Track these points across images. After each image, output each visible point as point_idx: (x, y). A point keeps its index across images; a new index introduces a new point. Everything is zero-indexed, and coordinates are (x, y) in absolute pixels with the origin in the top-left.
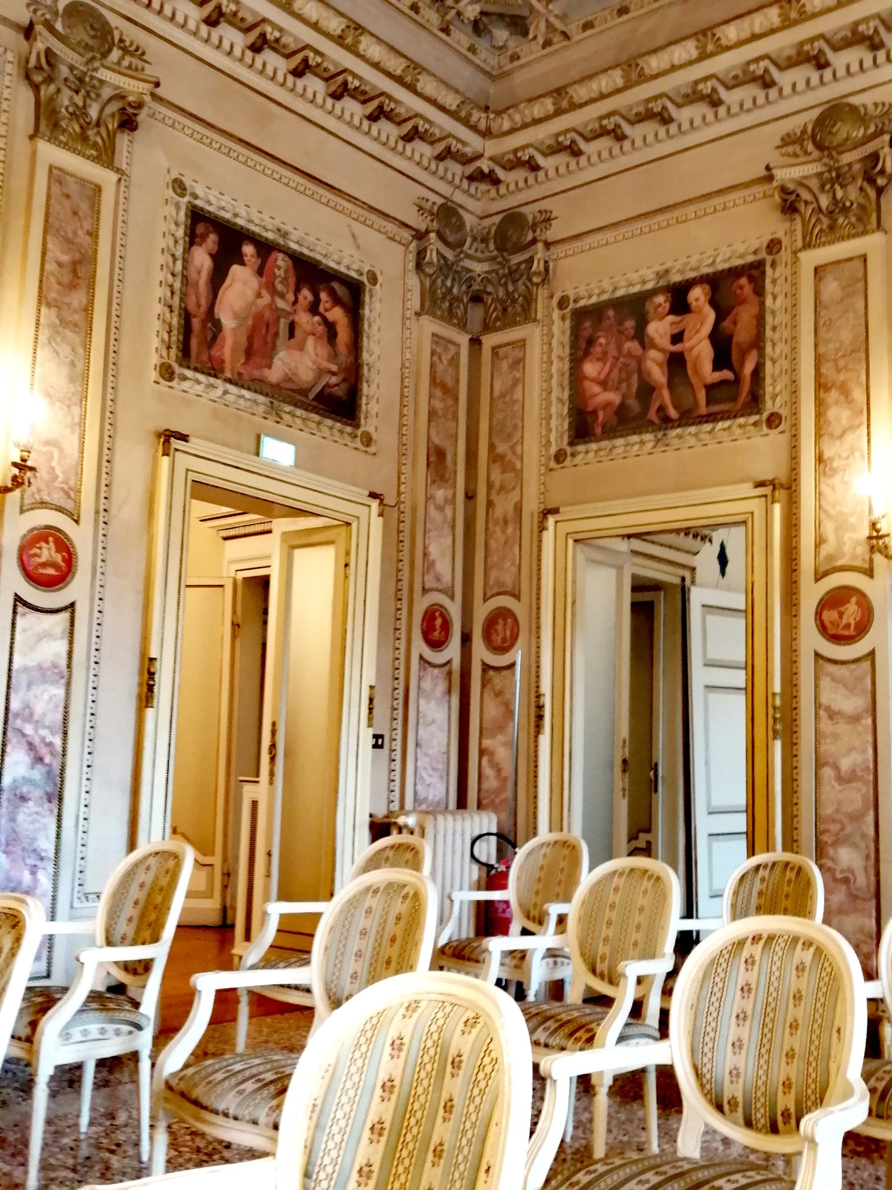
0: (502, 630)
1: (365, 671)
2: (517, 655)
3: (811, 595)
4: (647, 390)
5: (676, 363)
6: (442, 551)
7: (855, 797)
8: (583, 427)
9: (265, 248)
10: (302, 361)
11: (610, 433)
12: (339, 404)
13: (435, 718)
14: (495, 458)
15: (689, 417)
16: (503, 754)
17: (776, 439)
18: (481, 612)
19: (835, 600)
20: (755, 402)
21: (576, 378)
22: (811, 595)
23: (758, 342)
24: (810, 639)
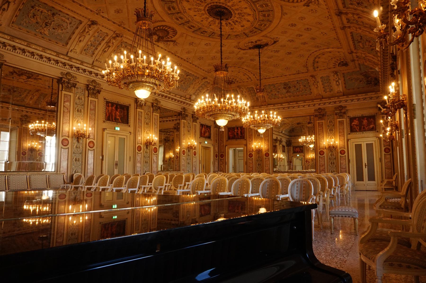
0: (222, 156)
1: (212, 160)
2: (224, 158)
3: (248, 154)
4: (235, 136)
5: (237, 134)
6: (217, 149)
7: (251, 169)
8: (229, 138)
9: (204, 125)
10: (207, 134)
11: (231, 139)
12: (209, 137)
13: (217, 163)
14: (221, 140)
15: (238, 138)
16: (223, 167)
17: (245, 141)
18: (220, 154)
19: (250, 154)
20: (244, 138)
21: (228, 134)
22: (248, 154)
23: (244, 133)
24: (248, 157)
